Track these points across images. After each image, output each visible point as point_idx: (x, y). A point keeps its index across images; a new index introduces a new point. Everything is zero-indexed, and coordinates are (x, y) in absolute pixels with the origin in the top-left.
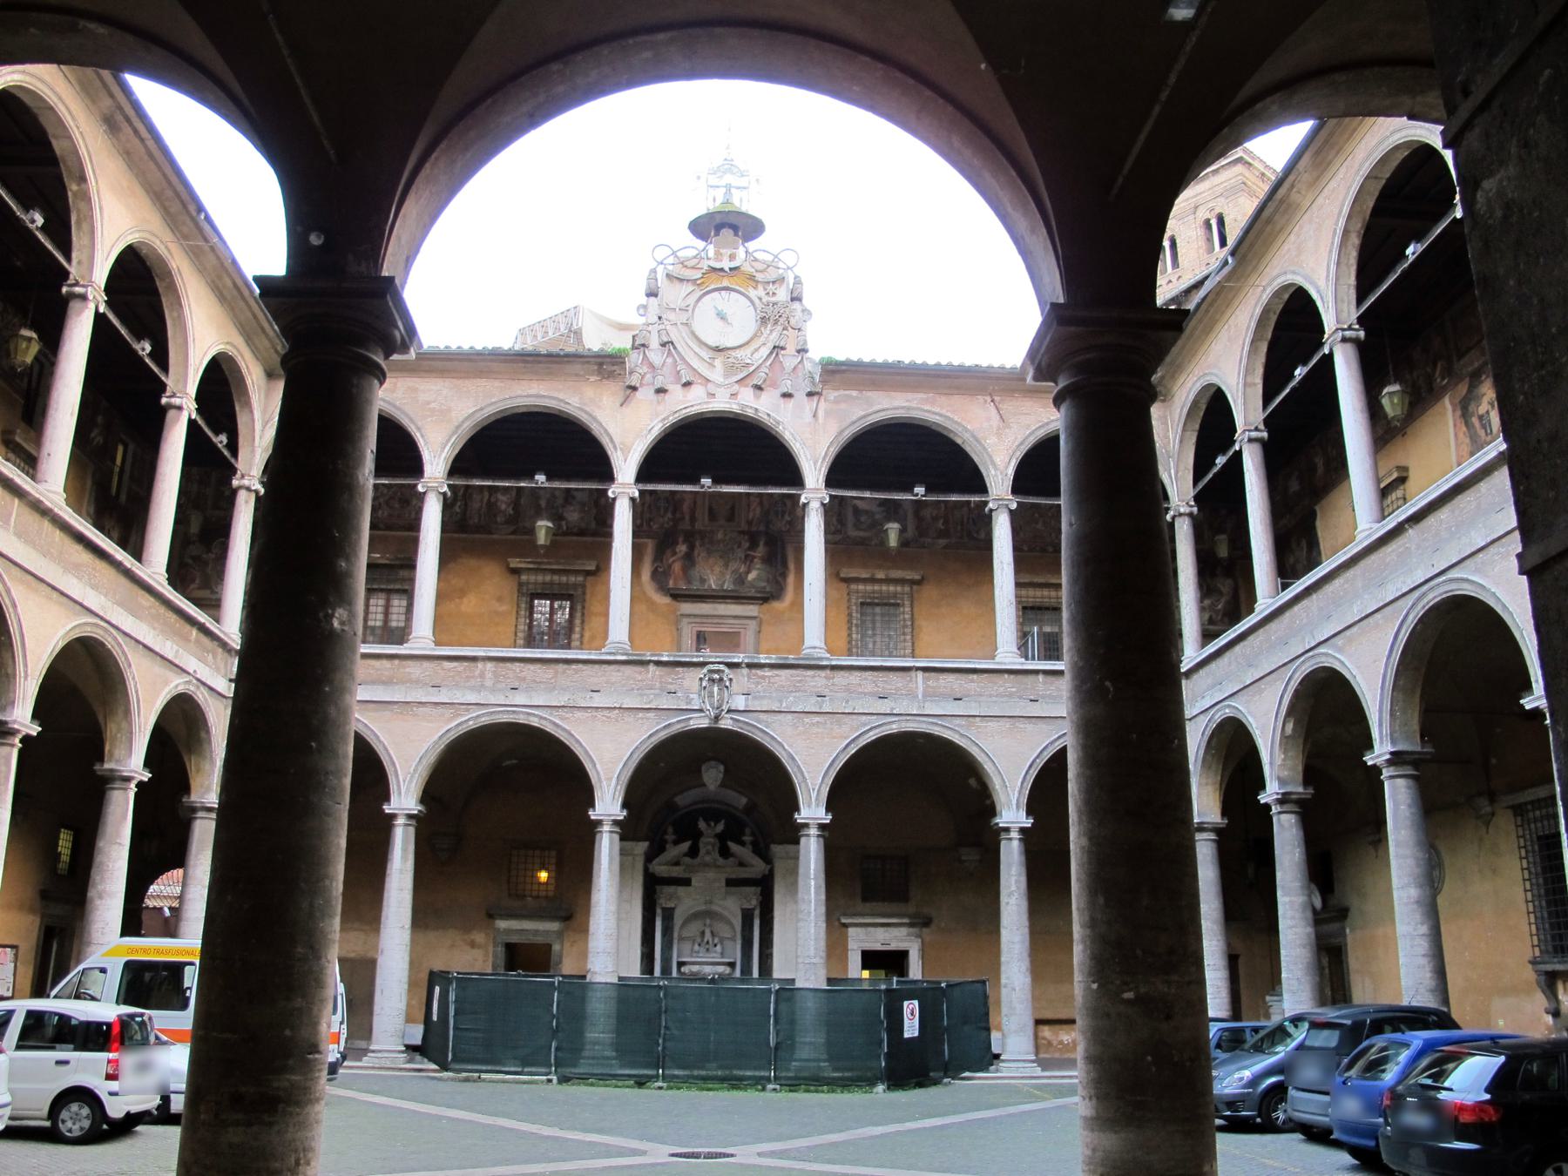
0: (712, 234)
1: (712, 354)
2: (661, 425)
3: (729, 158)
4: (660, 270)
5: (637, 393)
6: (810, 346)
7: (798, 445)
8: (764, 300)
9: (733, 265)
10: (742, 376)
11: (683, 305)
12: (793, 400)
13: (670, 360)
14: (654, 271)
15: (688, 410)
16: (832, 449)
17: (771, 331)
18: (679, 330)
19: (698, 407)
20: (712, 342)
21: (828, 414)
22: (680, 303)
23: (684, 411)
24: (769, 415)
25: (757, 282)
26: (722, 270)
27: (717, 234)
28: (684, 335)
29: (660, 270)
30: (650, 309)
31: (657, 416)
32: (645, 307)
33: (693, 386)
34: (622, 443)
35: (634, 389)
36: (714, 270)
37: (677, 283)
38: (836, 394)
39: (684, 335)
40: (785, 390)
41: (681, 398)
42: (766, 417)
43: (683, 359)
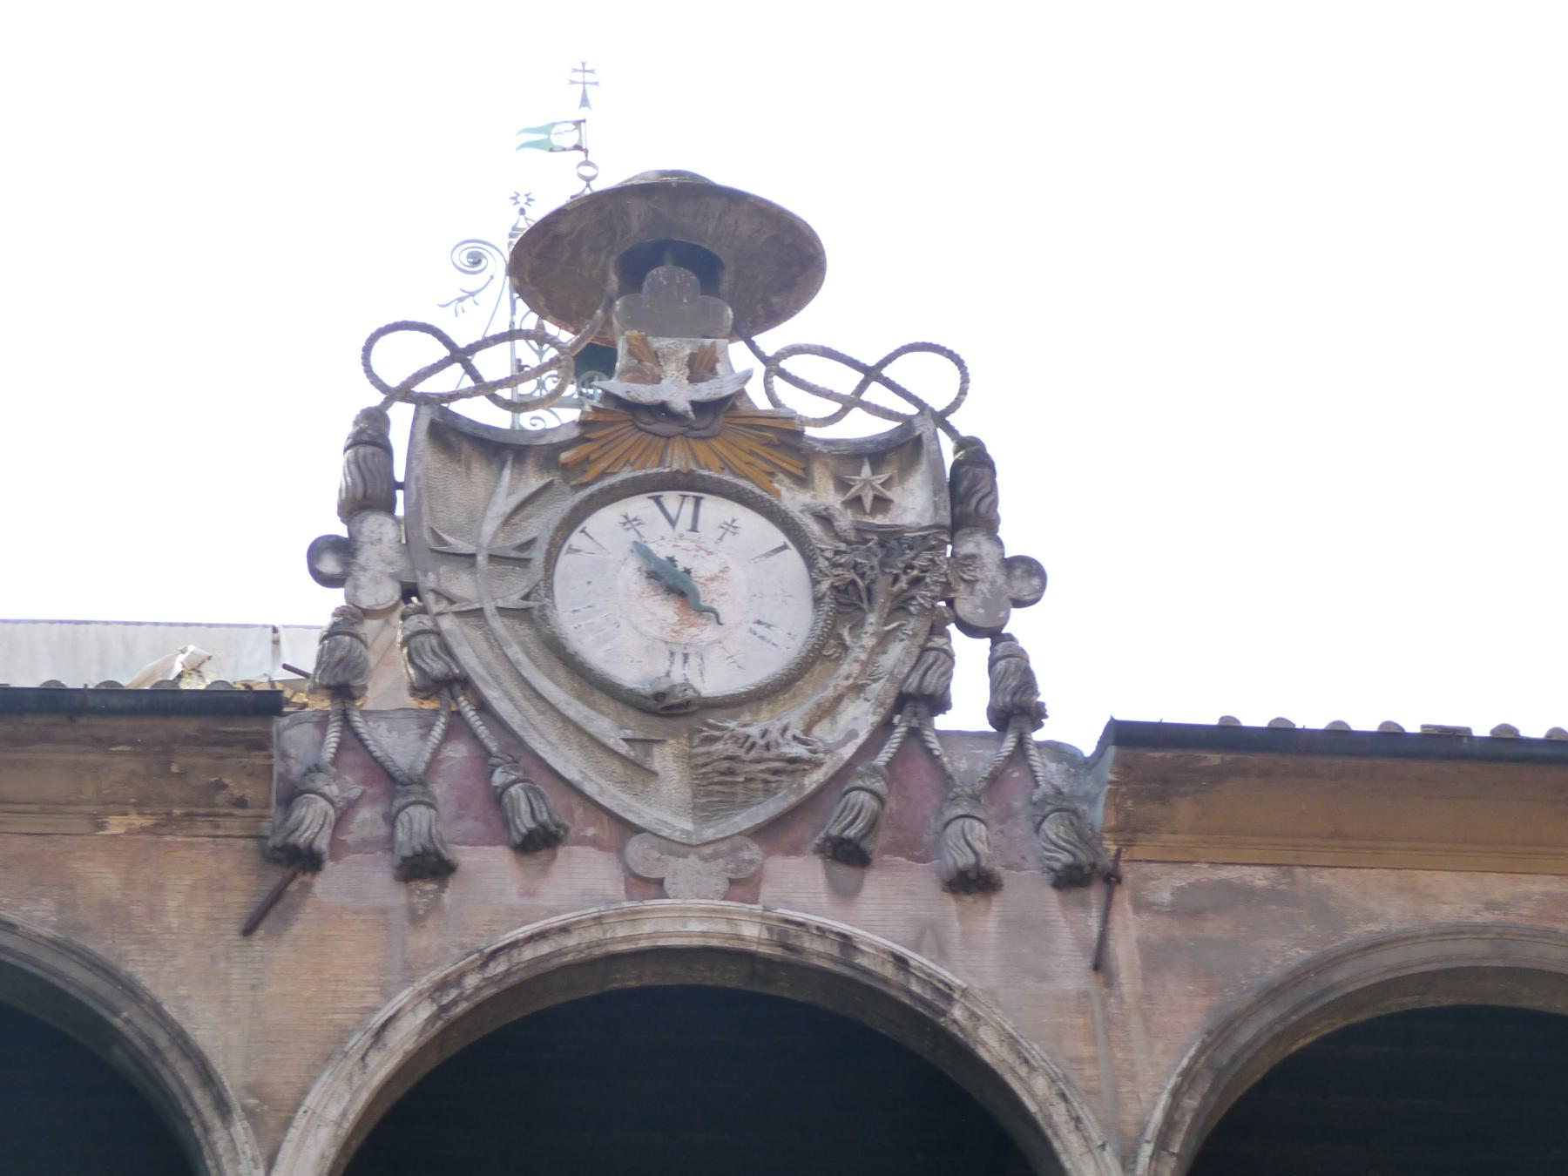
1: (636, 726)
2: (426, 1011)
4: (401, 418)
6: (1046, 693)
7: (1040, 1084)
9: (706, 391)
11: (506, 545)
13: (458, 752)
15: (545, 948)
16: (1191, 1102)
17: (884, 640)
18: (495, 643)
21: (1155, 958)
23: (528, 953)
24: (901, 962)
28: (515, 652)
29: (401, 418)
30: (368, 556)
31: (410, 973)
32: (343, 549)
33: (562, 852)
34: (251, 1089)
35: (306, 861)
36: (631, 408)
38: (1182, 878)
39: (515, 652)
40: (965, 859)
41: (512, 897)
42: (889, 971)
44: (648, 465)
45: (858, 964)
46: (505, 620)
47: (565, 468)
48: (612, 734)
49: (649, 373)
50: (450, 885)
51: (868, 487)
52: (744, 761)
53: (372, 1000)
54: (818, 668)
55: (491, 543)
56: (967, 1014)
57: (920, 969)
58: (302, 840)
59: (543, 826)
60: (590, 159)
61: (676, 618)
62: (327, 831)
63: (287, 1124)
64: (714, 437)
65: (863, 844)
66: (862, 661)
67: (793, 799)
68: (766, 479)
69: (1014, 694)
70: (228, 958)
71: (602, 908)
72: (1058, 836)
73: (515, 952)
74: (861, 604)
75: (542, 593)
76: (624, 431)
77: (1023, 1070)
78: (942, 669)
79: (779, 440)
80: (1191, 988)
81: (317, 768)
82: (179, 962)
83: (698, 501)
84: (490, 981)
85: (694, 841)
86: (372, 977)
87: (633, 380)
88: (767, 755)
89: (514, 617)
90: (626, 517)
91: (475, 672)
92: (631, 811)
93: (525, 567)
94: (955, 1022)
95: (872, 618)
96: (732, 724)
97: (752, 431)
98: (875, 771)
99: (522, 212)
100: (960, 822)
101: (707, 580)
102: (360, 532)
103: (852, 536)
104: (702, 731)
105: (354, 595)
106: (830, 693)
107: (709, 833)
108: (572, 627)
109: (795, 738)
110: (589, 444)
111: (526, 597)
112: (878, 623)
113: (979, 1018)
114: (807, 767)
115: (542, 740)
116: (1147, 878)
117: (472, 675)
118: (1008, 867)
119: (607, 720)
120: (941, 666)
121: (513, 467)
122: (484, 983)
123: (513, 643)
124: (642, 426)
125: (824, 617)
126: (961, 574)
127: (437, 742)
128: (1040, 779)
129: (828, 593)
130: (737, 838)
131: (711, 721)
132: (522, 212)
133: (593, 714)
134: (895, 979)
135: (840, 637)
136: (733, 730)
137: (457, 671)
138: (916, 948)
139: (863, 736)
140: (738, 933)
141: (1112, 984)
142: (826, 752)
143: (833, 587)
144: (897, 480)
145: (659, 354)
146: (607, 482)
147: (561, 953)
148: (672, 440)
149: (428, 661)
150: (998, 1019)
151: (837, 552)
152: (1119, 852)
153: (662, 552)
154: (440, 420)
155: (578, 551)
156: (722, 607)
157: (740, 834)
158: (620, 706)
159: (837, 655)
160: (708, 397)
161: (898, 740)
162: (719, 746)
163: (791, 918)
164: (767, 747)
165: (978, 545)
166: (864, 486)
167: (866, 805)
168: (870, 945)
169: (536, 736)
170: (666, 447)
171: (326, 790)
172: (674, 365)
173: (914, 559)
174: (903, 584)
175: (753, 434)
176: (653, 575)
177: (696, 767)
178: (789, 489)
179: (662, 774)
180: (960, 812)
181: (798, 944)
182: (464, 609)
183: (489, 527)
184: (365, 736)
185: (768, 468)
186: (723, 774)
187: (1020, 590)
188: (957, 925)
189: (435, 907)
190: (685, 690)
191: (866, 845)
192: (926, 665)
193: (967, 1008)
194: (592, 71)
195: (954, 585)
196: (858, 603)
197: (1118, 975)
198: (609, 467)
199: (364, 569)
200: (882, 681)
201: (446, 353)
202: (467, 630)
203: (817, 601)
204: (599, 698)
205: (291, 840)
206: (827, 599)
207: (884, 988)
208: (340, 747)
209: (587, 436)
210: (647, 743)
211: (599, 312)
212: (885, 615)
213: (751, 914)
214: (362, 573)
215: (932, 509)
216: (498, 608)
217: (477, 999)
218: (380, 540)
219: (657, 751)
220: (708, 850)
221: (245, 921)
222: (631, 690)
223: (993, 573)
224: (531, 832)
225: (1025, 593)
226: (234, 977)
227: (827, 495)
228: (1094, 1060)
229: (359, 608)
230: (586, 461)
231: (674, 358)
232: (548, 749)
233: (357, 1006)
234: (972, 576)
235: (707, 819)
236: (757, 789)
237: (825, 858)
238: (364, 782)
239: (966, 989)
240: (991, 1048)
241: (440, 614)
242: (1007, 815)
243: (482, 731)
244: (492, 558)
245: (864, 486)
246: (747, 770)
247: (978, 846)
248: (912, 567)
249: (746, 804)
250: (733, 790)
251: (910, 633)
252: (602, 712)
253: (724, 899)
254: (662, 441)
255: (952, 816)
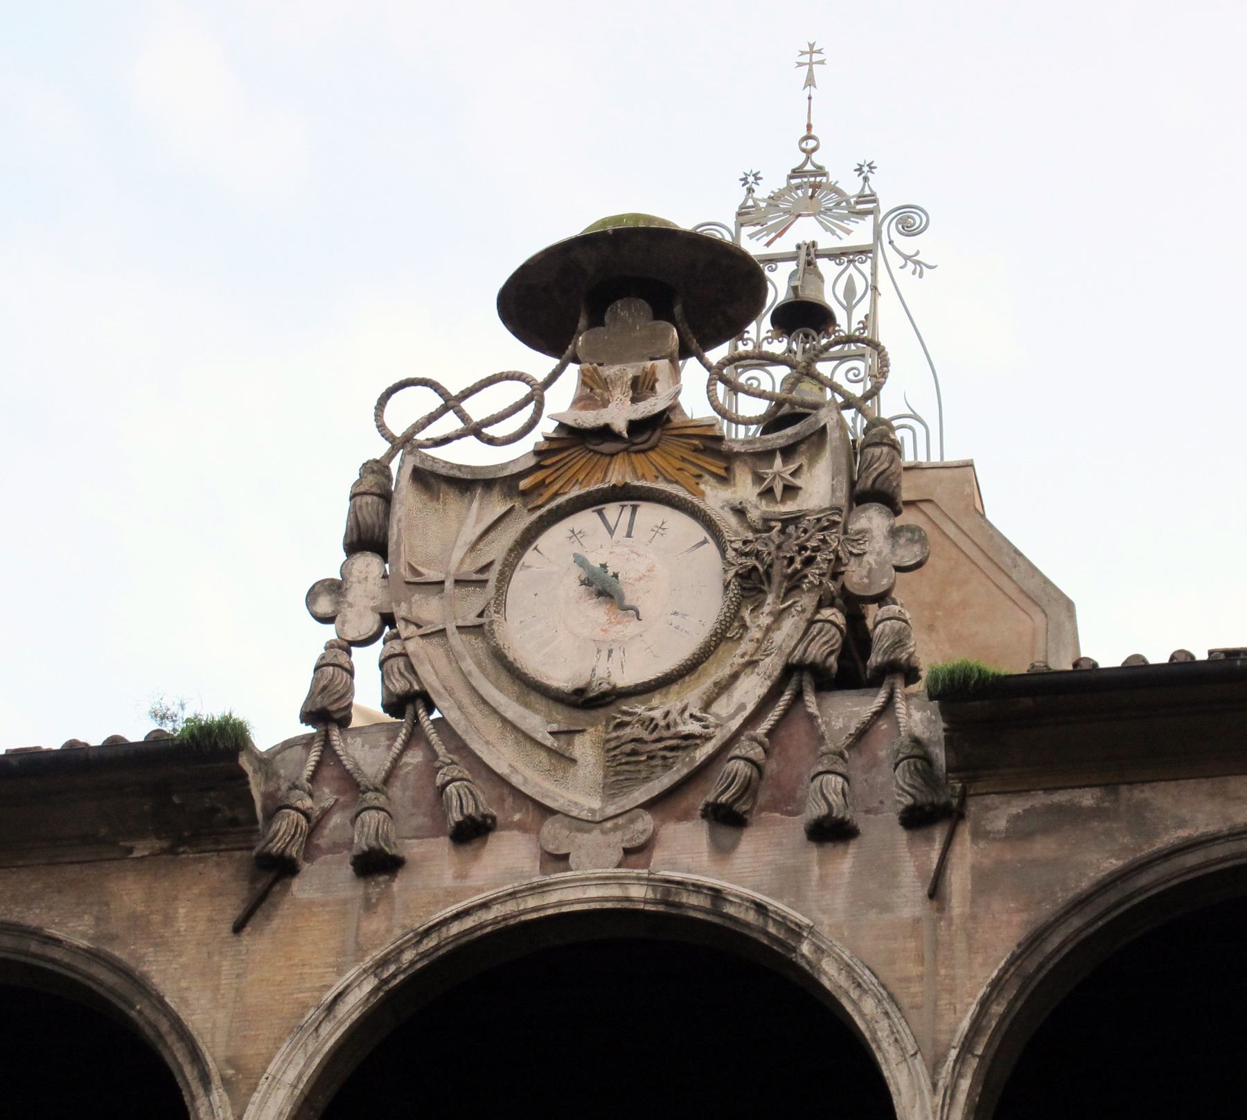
0: (582, 322)
1: (562, 718)
2: (369, 985)
3: (809, 167)
5: (296, 884)
7: (869, 1005)
8: (754, 515)
10: (665, 781)
11: (469, 569)
12: (853, 848)
13: (415, 757)
14: (376, 469)
15: (469, 923)
16: (998, 1009)
17: (779, 616)
18: (453, 657)
19: (510, 907)
20: (561, 677)
21: (984, 881)
22: (457, 561)
23: (455, 928)
24: (761, 908)
25: (729, 458)
26: (605, 433)
27: (596, 321)
28: (469, 665)
31: (360, 951)
32: (334, 588)
33: (493, 838)
37: (452, 502)
38: (1017, 806)
39: (469, 665)
40: (816, 810)
42: (751, 917)
43: (460, 747)
44: (593, 482)
45: (727, 913)
46: (464, 637)
47: (525, 494)
48: (541, 730)
49: (599, 399)
50: (399, 875)
51: (778, 479)
52: (646, 742)
53: (328, 979)
54: (722, 647)
55: (458, 568)
56: (813, 948)
57: (775, 913)
58: (275, 850)
59: (469, 817)
60: (813, 133)
61: (606, 618)
62: (300, 840)
63: (254, 1089)
64: (652, 448)
65: (736, 807)
66: (758, 640)
67: (685, 771)
68: (694, 480)
69: (885, 652)
70: (221, 953)
71: (516, 885)
72: (905, 782)
73: (444, 929)
74: (763, 587)
75: (492, 609)
76: (575, 454)
77: (855, 994)
78: (825, 639)
79: (704, 446)
80: (1012, 905)
81: (294, 787)
82: (183, 960)
83: (634, 508)
84: (423, 955)
85: (598, 818)
86: (331, 959)
87: (585, 408)
88: (666, 734)
89: (470, 633)
90: (573, 531)
91: (432, 687)
92: (547, 796)
93: (484, 587)
94: (803, 956)
95: (770, 599)
96: (640, 709)
97: (684, 440)
98: (754, 739)
99: (750, 190)
100: (820, 777)
101: (635, 580)
102: (350, 573)
103: (760, 526)
104: (616, 718)
105: (342, 630)
106: (727, 671)
107: (611, 810)
108: (518, 637)
109: (692, 716)
110: (543, 471)
111: (480, 615)
112: (774, 603)
113: (823, 951)
114: (698, 741)
115: (481, 741)
116: (988, 809)
117: (429, 691)
118: (868, 812)
119: (537, 717)
120: (824, 636)
121: (482, 498)
122: (418, 957)
123: (467, 656)
124: (591, 447)
125: (727, 603)
126: (850, 549)
127: (398, 752)
128: (902, 729)
129: (733, 580)
130: (637, 810)
131: (624, 708)
132: (750, 190)
133: (526, 712)
134: (755, 923)
135: (742, 618)
136: (640, 715)
137: (416, 687)
138: (778, 895)
139: (750, 708)
140: (627, 895)
141: (944, 909)
142: (717, 726)
143: (737, 575)
144: (805, 468)
145: (608, 381)
146: (553, 504)
147: (481, 926)
148: (615, 457)
149: (394, 681)
150: (838, 950)
151: (745, 542)
152: (964, 790)
153: (595, 560)
154: (421, 466)
155: (529, 567)
156: (646, 606)
157: (637, 807)
158: (550, 701)
159: (738, 636)
160: (643, 415)
161: (782, 707)
162: (628, 730)
163: (671, 878)
164: (668, 727)
165: (870, 519)
166: (774, 478)
167: (739, 773)
168: (736, 896)
169: (476, 737)
170: (609, 464)
171: (299, 804)
172: (619, 389)
173: (808, 540)
174: (797, 565)
175: (684, 443)
176: (586, 582)
177: (609, 751)
178: (713, 488)
179: (580, 761)
180: (820, 768)
181: (677, 900)
182: (429, 631)
183: (458, 554)
184: (340, 753)
185: (698, 472)
186: (629, 755)
187: (903, 557)
188: (816, 868)
189: (386, 896)
190: (600, 684)
191: (741, 807)
192: (810, 638)
193: (814, 944)
194: (819, 52)
195: (845, 561)
196: (759, 586)
197: (950, 900)
198: (561, 487)
199: (351, 605)
200: (773, 655)
201: (441, 402)
202: (430, 649)
203: (726, 587)
204: (534, 698)
205: (266, 850)
206: (732, 586)
207: (746, 931)
208: (319, 764)
209: (542, 463)
210: (571, 733)
211: (570, 347)
212: (782, 595)
213: (639, 878)
214: (350, 609)
215: (830, 491)
216: (458, 627)
217: (410, 972)
218: (366, 578)
219: (578, 739)
220: (609, 824)
221: (234, 920)
222: (557, 689)
223: (881, 544)
224: (458, 824)
225: (907, 559)
226: (224, 968)
227: (745, 489)
228: (921, 978)
229: (346, 640)
230: (542, 485)
231: (619, 383)
232: (484, 749)
233: (317, 985)
234: (862, 550)
235: (613, 796)
236: (657, 766)
237: (710, 822)
238: (338, 792)
239: (812, 927)
240: (831, 976)
241: (407, 639)
242: (874, 764)
243: (434, 738)
244: (457, 582)
245: (774, 478)
246: (648, 749)
247: (832, 798)
248: (806, 549)
249: (647, 779)
250: (637, 768)
251: (799, 609)
252: (536, 711)
253: (619, 866)
254: (607, 460)
255: (816, 772)
